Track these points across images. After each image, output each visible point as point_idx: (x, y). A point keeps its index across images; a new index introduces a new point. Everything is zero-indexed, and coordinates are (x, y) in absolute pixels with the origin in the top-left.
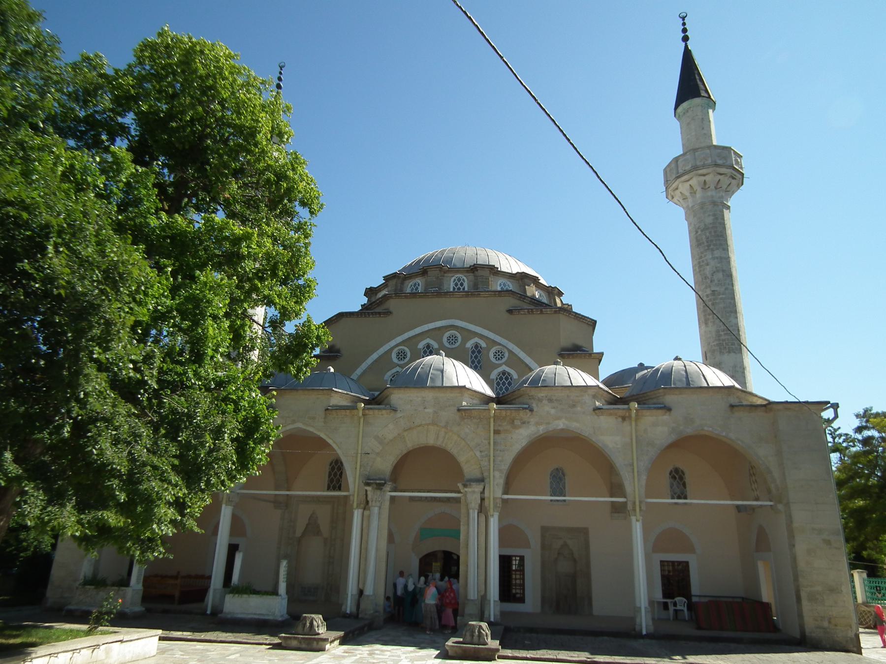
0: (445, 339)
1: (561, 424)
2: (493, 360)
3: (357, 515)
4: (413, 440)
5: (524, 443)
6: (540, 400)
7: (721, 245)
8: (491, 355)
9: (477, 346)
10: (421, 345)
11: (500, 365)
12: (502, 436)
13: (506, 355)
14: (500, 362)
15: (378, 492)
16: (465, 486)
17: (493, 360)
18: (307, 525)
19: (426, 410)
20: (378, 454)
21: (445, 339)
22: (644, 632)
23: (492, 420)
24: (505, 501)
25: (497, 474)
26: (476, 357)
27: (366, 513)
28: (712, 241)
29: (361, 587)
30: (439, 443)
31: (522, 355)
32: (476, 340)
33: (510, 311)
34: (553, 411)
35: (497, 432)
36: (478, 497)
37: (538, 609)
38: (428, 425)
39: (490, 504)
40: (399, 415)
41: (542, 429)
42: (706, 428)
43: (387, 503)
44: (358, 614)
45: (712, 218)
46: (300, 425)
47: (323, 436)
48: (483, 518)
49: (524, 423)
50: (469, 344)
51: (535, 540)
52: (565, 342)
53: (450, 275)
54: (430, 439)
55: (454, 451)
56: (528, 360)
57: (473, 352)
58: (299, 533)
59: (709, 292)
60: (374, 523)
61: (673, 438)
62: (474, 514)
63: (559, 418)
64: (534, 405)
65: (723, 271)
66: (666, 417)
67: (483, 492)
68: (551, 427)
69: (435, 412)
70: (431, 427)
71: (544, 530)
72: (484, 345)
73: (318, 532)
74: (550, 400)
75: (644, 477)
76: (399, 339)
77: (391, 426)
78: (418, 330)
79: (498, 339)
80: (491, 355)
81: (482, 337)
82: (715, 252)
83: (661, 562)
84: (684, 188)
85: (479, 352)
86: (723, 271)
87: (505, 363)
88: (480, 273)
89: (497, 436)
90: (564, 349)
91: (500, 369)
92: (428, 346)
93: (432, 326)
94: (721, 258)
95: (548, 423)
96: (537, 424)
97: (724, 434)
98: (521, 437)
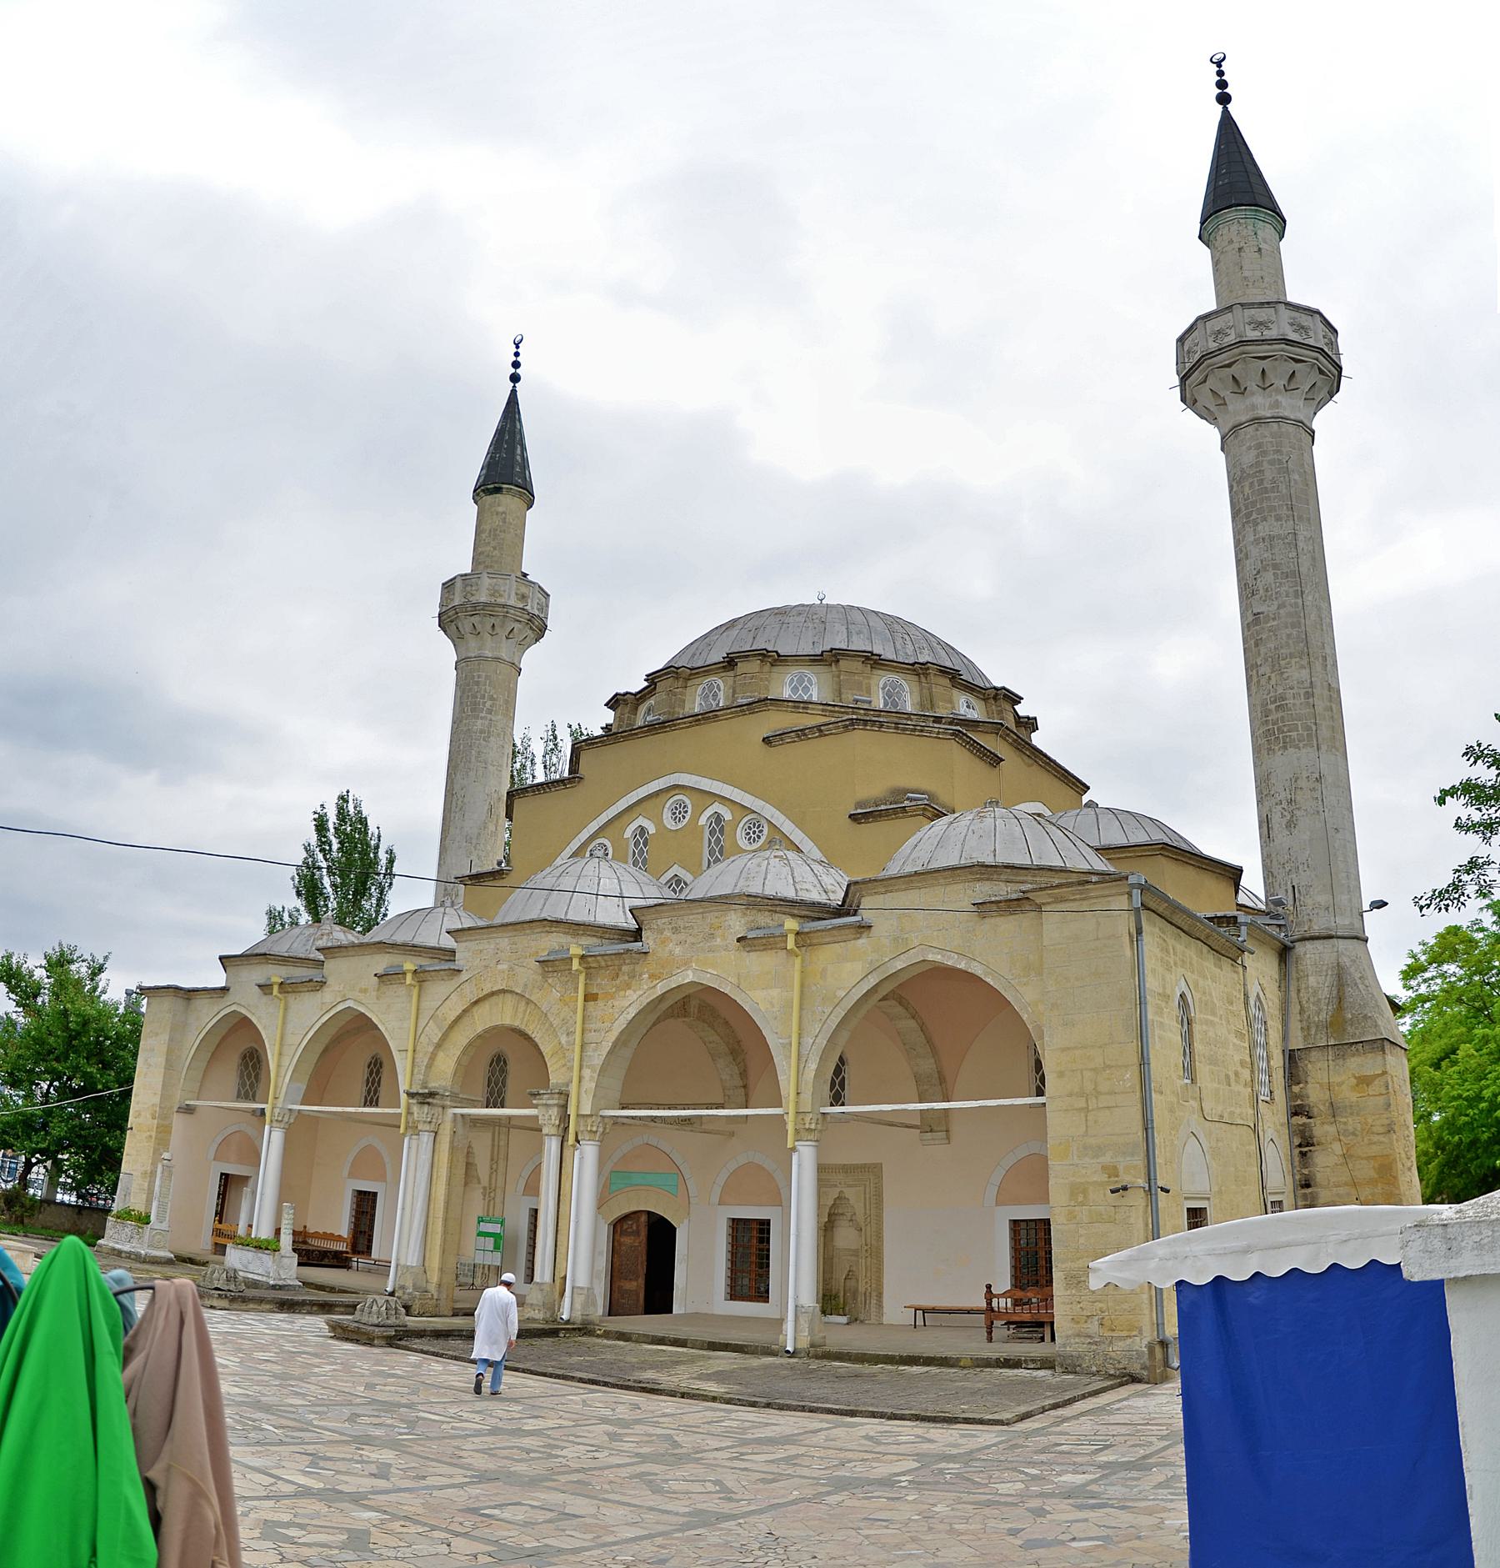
0: (667, 815)
1: (689, 977)
2: (743, 843)
4: (483, 1019)
5: (632, 1012)
6: (661, 932)
7: (1272, 509)
8: (740, 834)
9: (718, 818)
10: (628, 834)
12: (600, 1003)
14: (755, 846)
17: (743, 843)
20: (438, 1046)
21: (667, 815)
23: (582, 978)
26: (718, 841)
28: (1254, 503)
30: (516, 1023)
31: (787, 827)
32: (717, 807)
33: (767, 741)
34: (677, 950)
35: (589, 997)
36: (554, 1112)
38: (503, 991)
40: (464, 976)
42: (930, 957)
45: (1253, 453)
46: (349, 1004)
47: (375, 1020)
50: (703, 821)
52: (873, 788)
53: (696, 681)
54: (504, 1014)
56: (797, 836)
57: (712, 833)
59: (1251, 618)
61: (872, 981)
62: (552, 1146)
63: (686, 964)
65: (1276, 566)
66: (862, 941)
67: (565, 1107)
69: (511, 969)
70: (509, 996)
72: (727, 816)
74: (676, 930)
75: (813, 1066)
76: (594, 826)
78: (622, 804)
79: (747, 800)
80: (740, 834)
82: (1260, 527)
84: (1205, 398)
85: (722, 831)
86: (1276, 566)
88: (742, 667)
90: (859, 805)
92: (642, 830)
93: (643, 792)
94: (1272, 538)
96: (652, 976)
97: (962, 966)
98: (629, 1002)
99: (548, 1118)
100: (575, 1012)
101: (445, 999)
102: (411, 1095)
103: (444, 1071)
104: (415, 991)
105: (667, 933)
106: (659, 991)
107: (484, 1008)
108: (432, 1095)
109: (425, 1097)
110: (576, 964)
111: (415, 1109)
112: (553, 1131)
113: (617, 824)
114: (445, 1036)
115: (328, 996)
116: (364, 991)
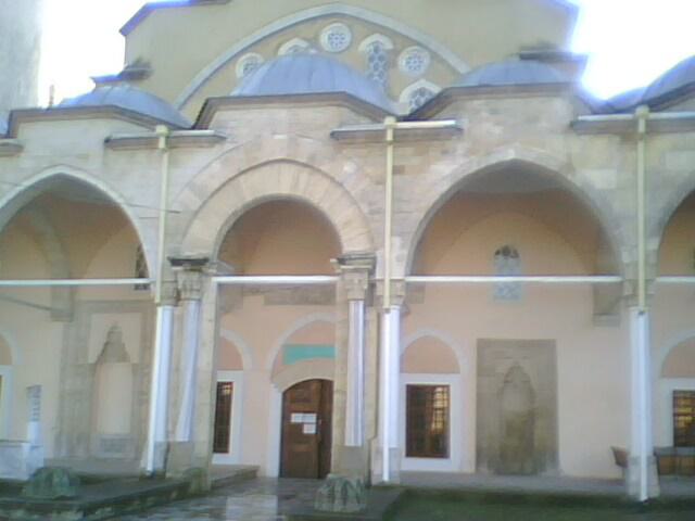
1: (510, 154)
3: (163, 316)
5: (445, 187)
11: (416, 80)
13: (426, 61)
15: (195, 276)
16: (342, 261)
18: (107, 344)
19: (278, 137)
20: (196, 213)
22: (643, 497)
24: (408, 284)
25: (397, 241)
27: (178, 310)
29: (170, 428)
34: (497, 130)
35: (397, 170)
37: (470, 468)
39: (385, 291)
40: (228, 146)
41: (475, 165)
43: (211, 296)
44: (164, 473)
47: (102, 186)
48: (372, 316)
49: (445, 152)
51: (466, 362)
55: (325, 207)
58: (92, 358)
60: (190, 325)
62: (357, 310)
64: (465, 123)
67: (372, 272)
68: (493, 160)
70: (285, 167)
71: (483, 346)
73: (124, 358)
74: (494, 112)
77: (216, 166)
81: (383, 30)
83: (675, 392)
87: (425, 76)
89: (397, 177)
91: (416, 86)
95: (488, 154)
96: (470, 152)
98: (443, 173)
99: (359, 283)
100: (381, 182)
101: (203, 166)
102: (175, 262)
103: (204, 237)
104: (166, 156)
105: (484, 114)
106: (474, 168)
107: (255, 176)
108: (204, 261)
109: (197, 265)
110: (389, 137)
111: (182, 278)
112: (361, 295)
113: (274, 43)
114: (205, 203)
115: (25, 162)
116: (85, 157)
